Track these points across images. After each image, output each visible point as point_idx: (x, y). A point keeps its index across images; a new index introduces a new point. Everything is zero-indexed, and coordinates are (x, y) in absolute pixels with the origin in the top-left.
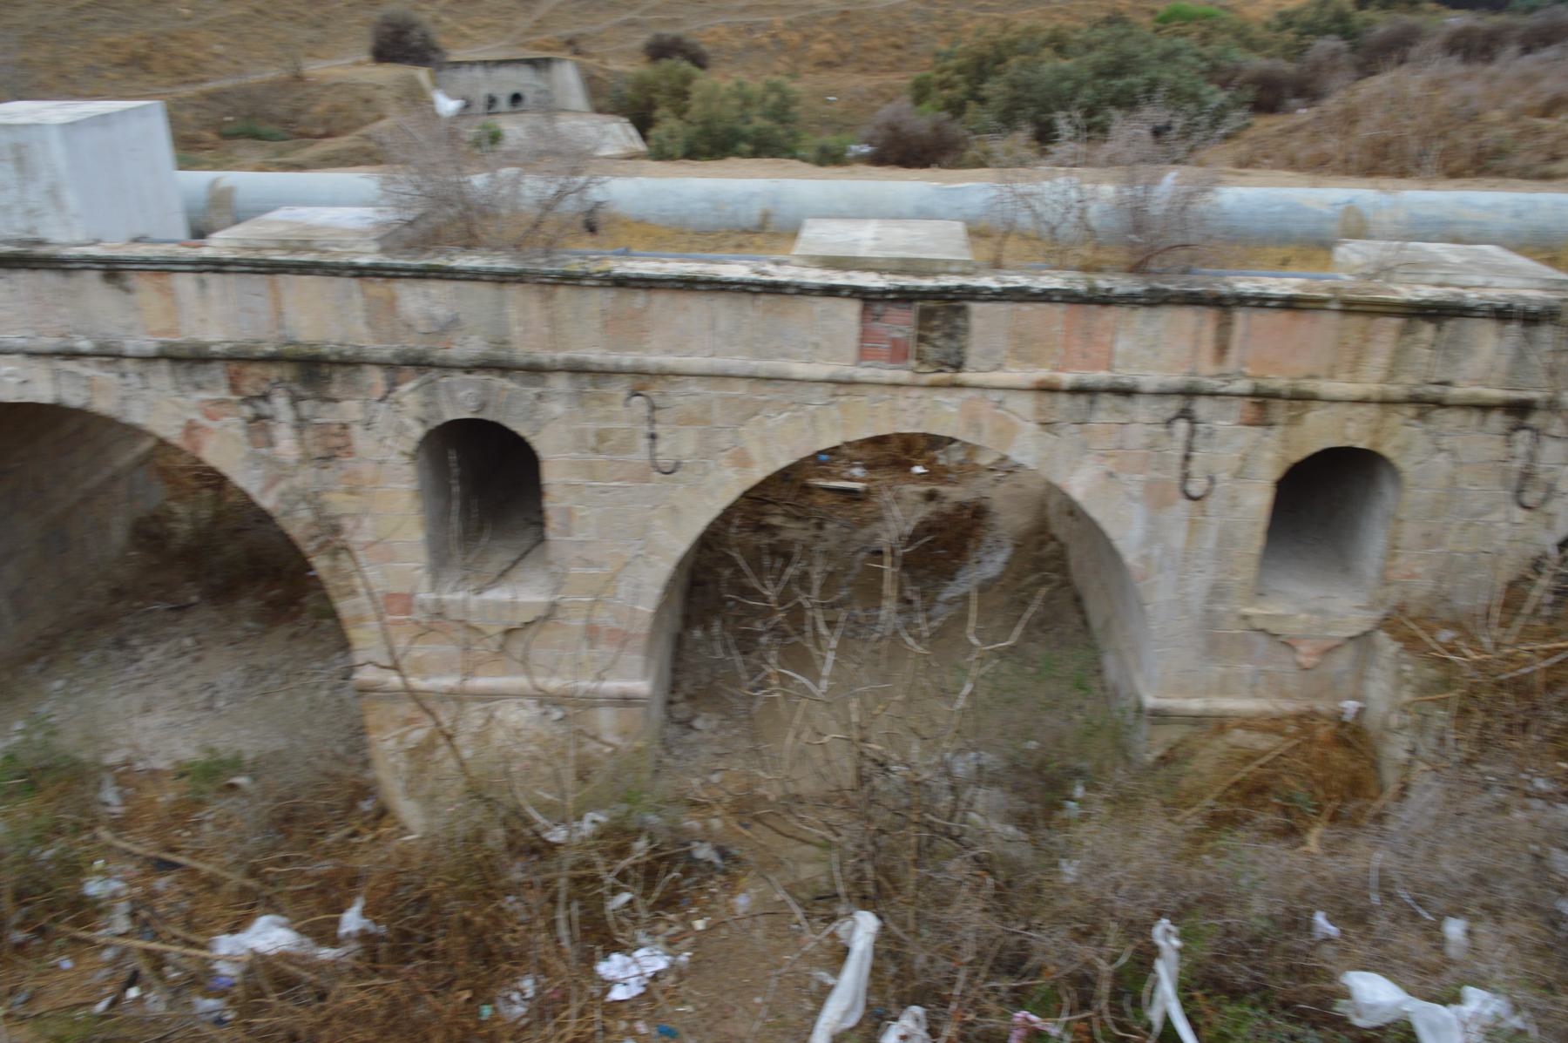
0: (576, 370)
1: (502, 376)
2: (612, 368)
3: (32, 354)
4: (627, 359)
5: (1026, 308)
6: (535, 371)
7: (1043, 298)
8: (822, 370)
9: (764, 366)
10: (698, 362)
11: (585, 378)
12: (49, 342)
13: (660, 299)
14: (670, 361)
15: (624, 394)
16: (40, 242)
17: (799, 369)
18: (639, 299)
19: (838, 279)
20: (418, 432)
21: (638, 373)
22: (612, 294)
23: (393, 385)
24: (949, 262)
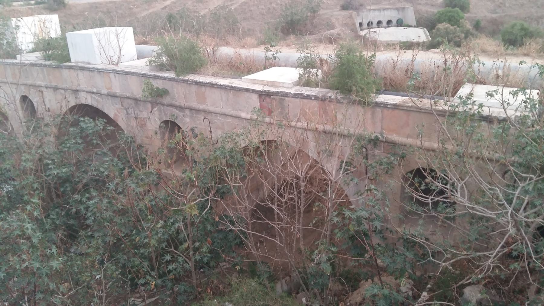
0: (191, 109)
1: (175, 109)
2: (193, 108)
3: (87, 92)
4: (201, 107)
5: (305, 101)
6: (181, 108)
7: (308, 98)
8: (249, 116)
9: (234, 113)
10: (218, 110)
11: (193, 111)
12: (89, 89)
13: (208, 89)
14: (212, 109)
15: (203, 118)
16: (89, 64)
17: (243, 115)
18: (203, 89)
19: (250, 87)
20: (159, 123)
21: (205, 111)
22: (197, 86)
23: (152, 108)
24: (283, 83)
